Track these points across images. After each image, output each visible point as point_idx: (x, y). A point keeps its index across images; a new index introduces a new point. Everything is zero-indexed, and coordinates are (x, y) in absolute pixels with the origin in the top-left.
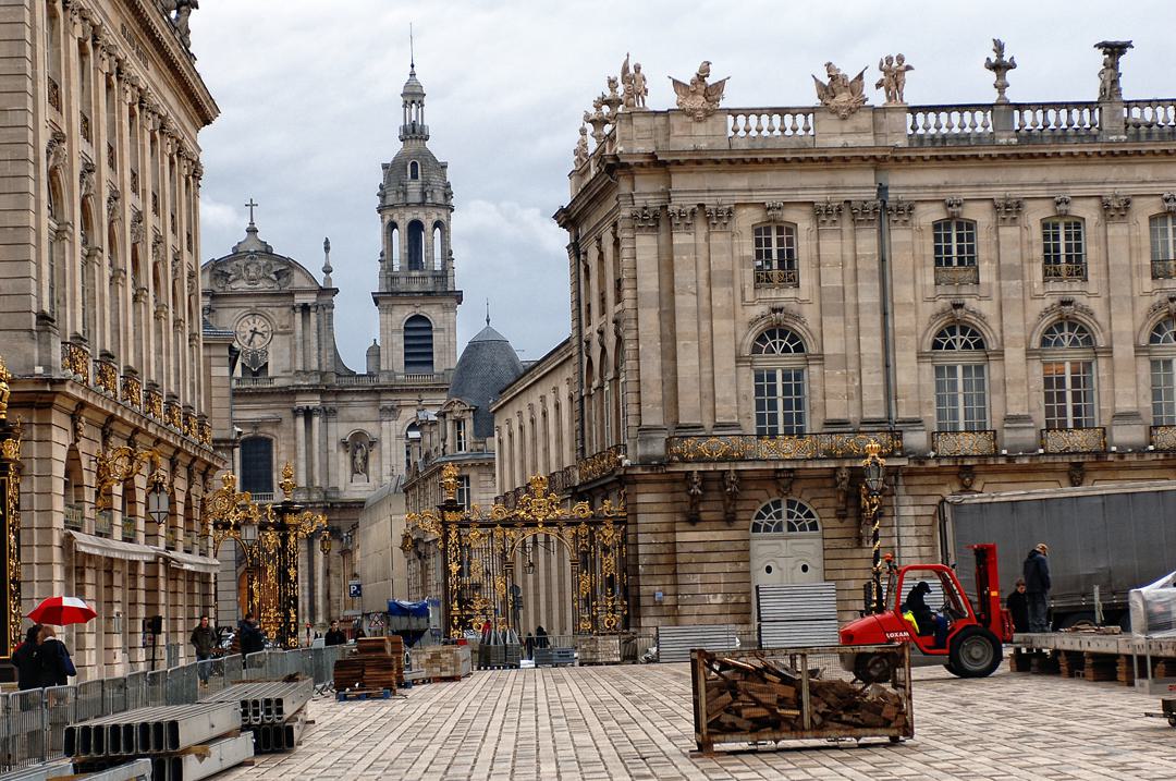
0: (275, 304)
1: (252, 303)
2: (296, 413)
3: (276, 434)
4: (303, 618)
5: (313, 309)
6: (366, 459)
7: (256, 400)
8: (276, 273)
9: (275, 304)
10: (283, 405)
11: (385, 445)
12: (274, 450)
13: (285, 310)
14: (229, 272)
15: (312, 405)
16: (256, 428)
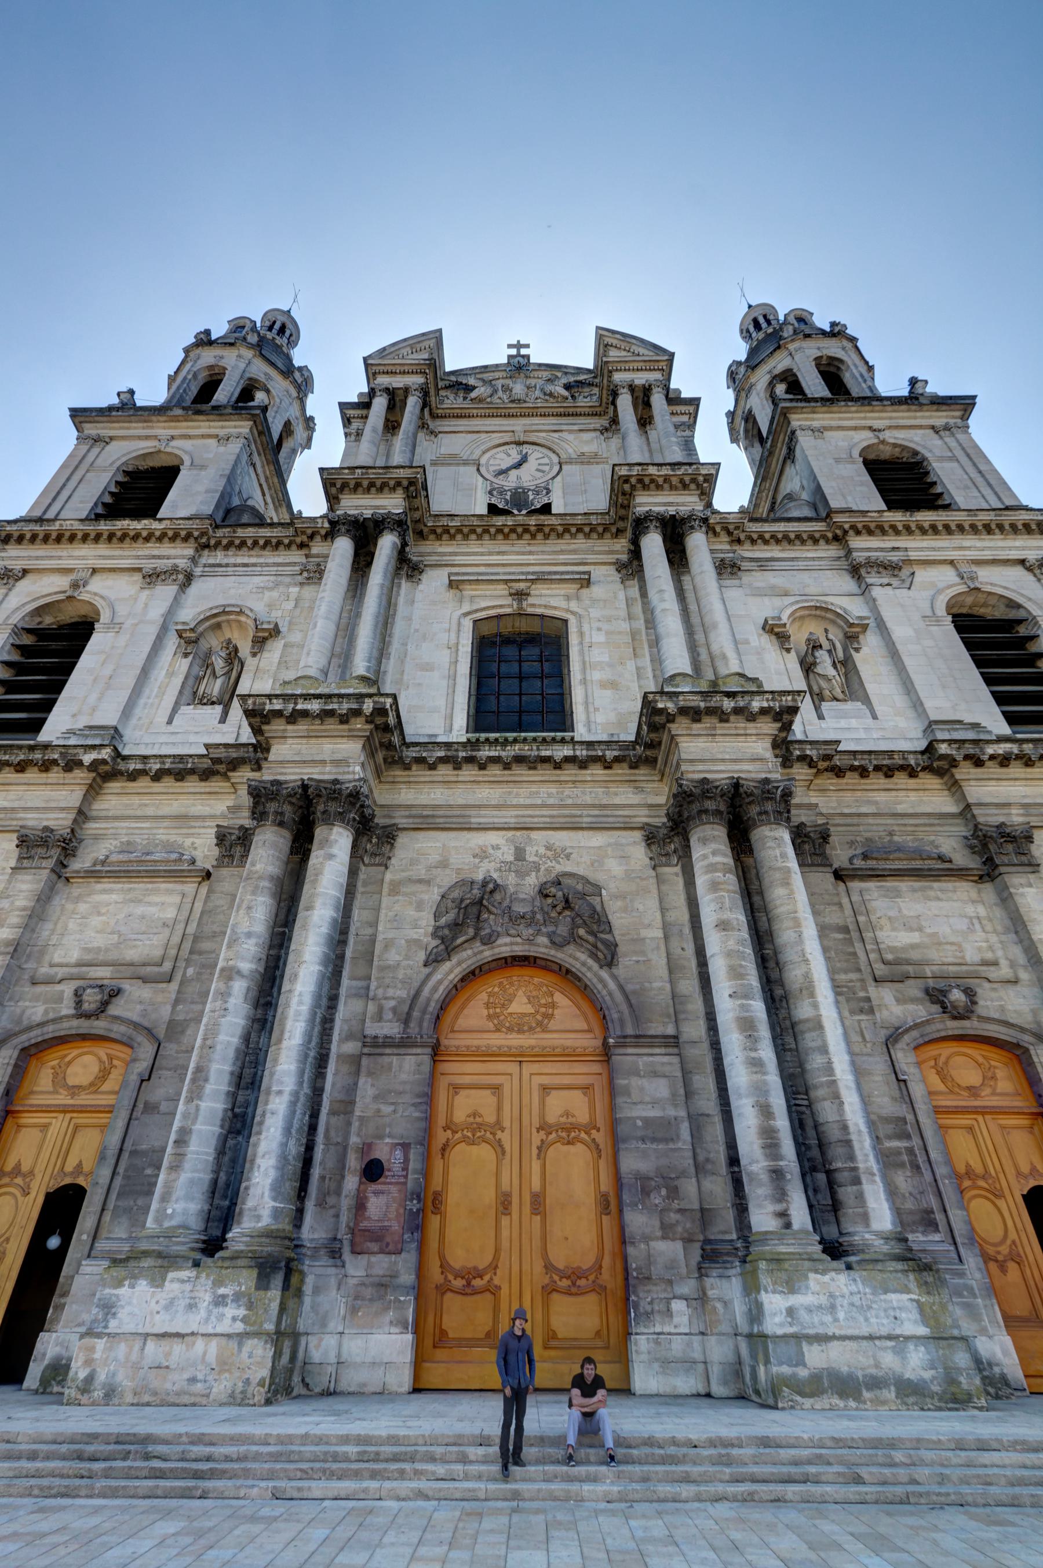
0: (564, 427)
1: (519, 425)
2: (640, 525)
3: (574, 605)
4: (781, 1195)
5: (655, 390)
6: (846, 665)
7: (516, 549)
8: (567, 387)
9: (564, 427)
10: (591, 558)
11: (900, 632)
12: (573, 639)
13: (587, 436)
14: (472, 381)
15: (684, 510)
16: (520, 595)
